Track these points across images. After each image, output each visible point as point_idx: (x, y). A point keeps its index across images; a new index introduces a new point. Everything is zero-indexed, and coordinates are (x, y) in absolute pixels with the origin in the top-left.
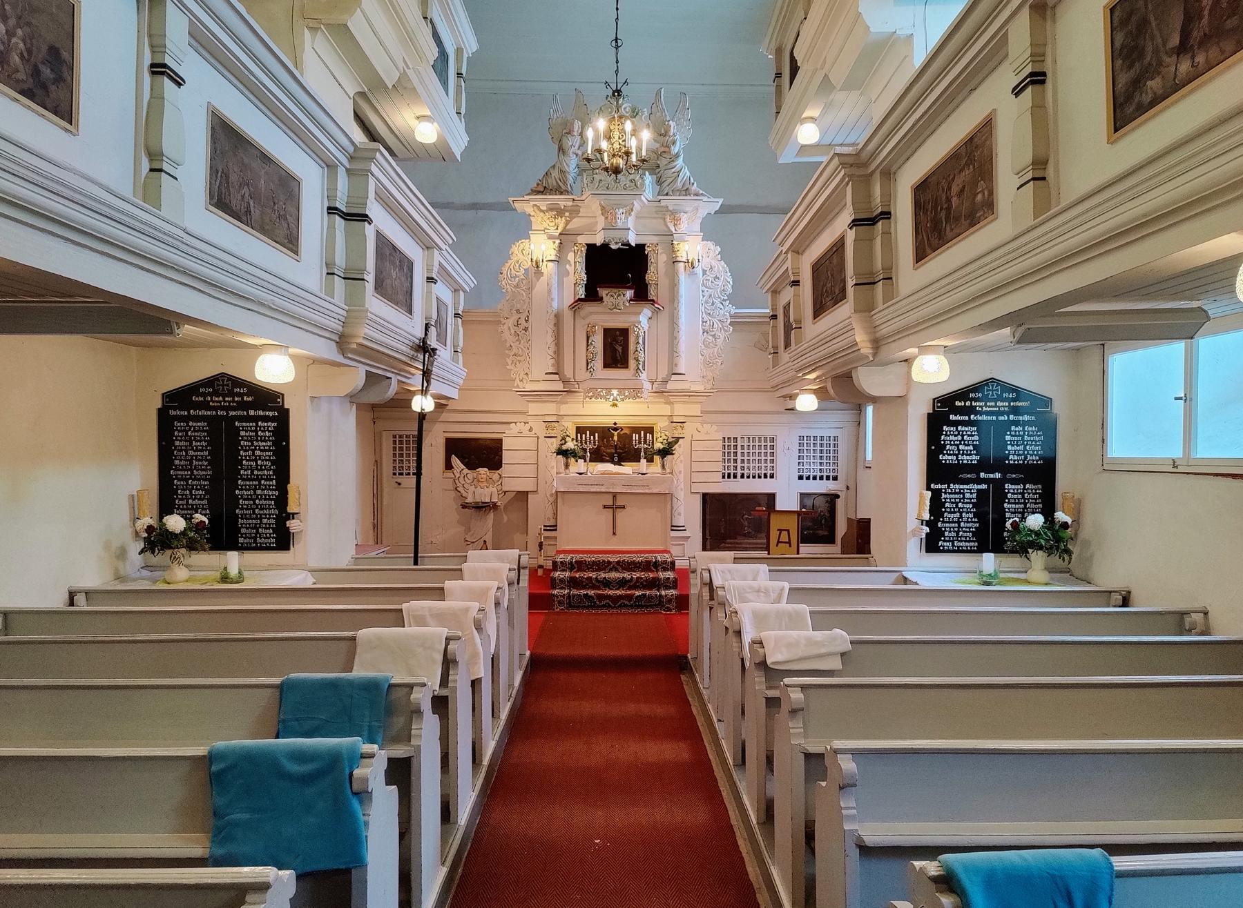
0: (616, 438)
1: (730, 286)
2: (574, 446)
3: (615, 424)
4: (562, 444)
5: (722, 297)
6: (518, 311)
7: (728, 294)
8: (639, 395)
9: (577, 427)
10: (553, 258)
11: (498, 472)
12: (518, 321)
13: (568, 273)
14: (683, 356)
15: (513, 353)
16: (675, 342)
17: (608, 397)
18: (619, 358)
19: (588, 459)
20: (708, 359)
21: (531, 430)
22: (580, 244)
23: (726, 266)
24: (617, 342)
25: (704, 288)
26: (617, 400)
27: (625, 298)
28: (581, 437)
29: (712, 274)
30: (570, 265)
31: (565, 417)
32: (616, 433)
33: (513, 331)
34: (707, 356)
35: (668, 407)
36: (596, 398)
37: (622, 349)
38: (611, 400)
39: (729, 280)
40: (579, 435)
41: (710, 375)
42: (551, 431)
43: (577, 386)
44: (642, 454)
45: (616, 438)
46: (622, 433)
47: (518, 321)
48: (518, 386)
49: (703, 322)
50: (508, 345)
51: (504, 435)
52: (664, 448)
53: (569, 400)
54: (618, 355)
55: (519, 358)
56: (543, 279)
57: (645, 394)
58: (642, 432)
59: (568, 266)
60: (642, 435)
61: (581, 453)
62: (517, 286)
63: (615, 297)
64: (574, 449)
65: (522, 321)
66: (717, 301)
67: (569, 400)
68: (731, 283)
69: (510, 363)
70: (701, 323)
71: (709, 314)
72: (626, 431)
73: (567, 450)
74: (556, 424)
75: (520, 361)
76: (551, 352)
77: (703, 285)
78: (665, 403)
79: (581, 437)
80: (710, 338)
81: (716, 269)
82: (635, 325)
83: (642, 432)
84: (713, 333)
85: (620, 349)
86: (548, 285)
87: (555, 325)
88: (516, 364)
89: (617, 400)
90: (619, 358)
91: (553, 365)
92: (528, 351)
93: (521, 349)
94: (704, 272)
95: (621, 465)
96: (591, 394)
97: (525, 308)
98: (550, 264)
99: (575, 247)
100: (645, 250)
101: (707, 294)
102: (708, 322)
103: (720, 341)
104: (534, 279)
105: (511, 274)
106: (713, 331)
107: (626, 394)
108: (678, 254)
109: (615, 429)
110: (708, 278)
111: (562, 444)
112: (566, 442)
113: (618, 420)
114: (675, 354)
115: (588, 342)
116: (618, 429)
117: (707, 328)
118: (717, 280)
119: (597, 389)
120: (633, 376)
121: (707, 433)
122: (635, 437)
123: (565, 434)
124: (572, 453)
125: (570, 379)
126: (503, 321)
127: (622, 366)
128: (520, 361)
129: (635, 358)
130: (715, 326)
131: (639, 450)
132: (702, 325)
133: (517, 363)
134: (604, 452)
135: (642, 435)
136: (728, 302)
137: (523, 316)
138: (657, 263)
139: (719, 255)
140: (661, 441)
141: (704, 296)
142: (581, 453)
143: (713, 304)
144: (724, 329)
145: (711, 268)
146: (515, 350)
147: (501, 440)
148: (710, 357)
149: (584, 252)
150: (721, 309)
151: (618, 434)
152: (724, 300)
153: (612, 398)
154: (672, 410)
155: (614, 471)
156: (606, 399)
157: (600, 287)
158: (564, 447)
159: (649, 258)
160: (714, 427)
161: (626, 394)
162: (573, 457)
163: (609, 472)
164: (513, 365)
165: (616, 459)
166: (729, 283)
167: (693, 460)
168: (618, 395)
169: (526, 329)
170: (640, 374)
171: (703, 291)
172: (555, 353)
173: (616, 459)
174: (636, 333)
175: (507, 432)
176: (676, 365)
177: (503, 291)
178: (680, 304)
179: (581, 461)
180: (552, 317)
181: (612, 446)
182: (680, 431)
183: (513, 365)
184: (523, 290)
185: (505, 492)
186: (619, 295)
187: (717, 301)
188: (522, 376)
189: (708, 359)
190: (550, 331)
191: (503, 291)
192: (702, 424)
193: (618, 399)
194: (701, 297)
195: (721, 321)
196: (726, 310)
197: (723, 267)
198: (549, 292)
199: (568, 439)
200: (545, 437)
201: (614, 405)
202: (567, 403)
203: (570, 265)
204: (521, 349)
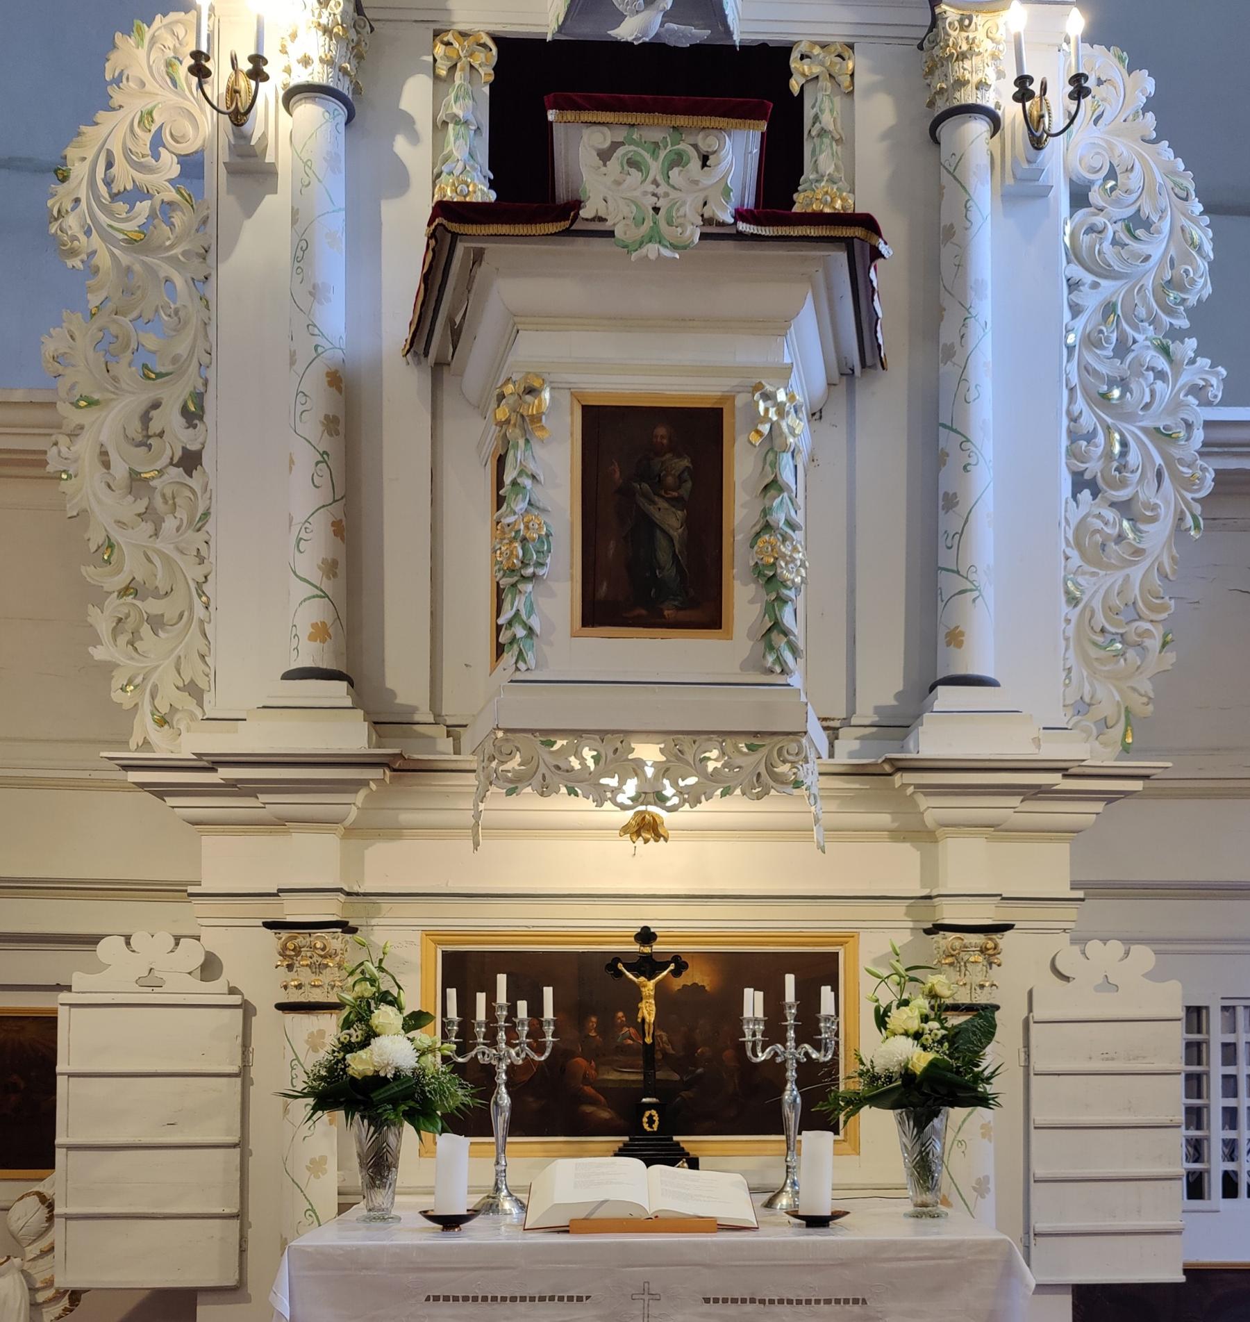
0: (648, 1011)
1: (1203, 266)
2: (422, 1053)
3: (646, 936)
4: (348, 1047)
5: (1166, 319)
6: (148, 374)
7: (1192, 300)
8: (783, 769)
9: (445, 954)
10: (318, 74)
11: (38, 1187)
12: (146, 419)
13: (399, 180)
14: (989, 592)
15: (121, 581)
16: (949, 522)
17: (613, 782)
18: (668, 572)
19: (501, 1122)
20: (1100, 620)
21: (210, 968)
22: (464, 35)
23: (1181, 165)
24: (658, 483)
25: (1077, 272)
26: (660, 799)
27: (709, 179)
28: (466, 1008)
29: (1118, 203)
30: (414, 138)
31: (385, 904)
32: (649, 987)
33: (120, 470)
34: (1097, 604)
35: (908, 854)
36: (545, 790)
37: (688, 523)
38: (621, 798)
39: (1197, 234)
40: (452, 993)
41: (1108, 699)
42: (305, 976)
43: (446, 744)
44: (791, 1093)
45: (648, 1011)
46: (678, 983)
47: (146, 419)
48: (146, 745)
49: (1073, 436)
50: (97, 539)
51: (64, 997)
52: (933, 1064)
53: (405, 817)
54: (664, 556)
55: (152, 606)
56: (276, 206)
57: (810, 773)
58: (790, 980)
59: (401, 145)
60: (790, 995)
61: (459, 1096)
62: (138, 243)
63: (655, 167)
64: (418, 1074)
65: (170, 419)
66: (1144, 337)
67: (405, 817)
68: (1208, 248)
69: (102, 622)
70: (1064, 442)
71: (1105, 396)
72: (696, 976)
73: (376, 1081)
74: (335, 940)
75: (157, 623)
76: (310, 561)
77: (1075, 255)
78: (898, 835)
79: (466, 1008)
80: (1110, 514)
81: (1134, 180)
82: (758, 387)
83: (790, 980)
84: (1122, 494)
85: (672, 521)
86: (294, 221)
87: (331, 424)
88: (135, 636)
89: (660, 799)
90: (668, 572)
91: (320, 633)
92: (194, 573)
93: (167, 559)
94: (1079, 198)
95: (672, 1156)
96: (514, 764)
97: (182, 348)
98: (309, 112)
99: (440, 50)
100: (789, 74)
101: (1091, 301)
102: (1101, 438)
103: (1157, 535)
104: (229, 203)
105: (108, 183)
106: (1123, 484)
107: (711, 766)
108: (969, 70)
109: (648, 965)
110: (1099, 220)
111: (348, 1047)
112: (371, 1035)
113: (659, 918)
114: (948, 583)
115: (500, 484)
116: (664, 966)
117: (1093, 468)
118: (1140, 232)
119: (547, 736)
120: (745, 666)
121: (1108, 985)
122: (753, 1003)
123: (367, 990)
124: (407, 1096)
125: (414, 710)
126: (75, 417)
127: (683, 615)
128: (157, 623)
129: (758, 570)
130: (1134, 458)
131: (775, 1069)
132: (1072, 453)
133: (146, 629)
134: (586, 1080)
135: (790, 995)
136: (1192, 343)
137: (174, 396)
138: (845, 141)
139: (1150, 116)
140: (915, 1025)
141: (1076, 310)
142: (459, 1096)
143: (1122, 349)
144: (1178, 479)
145: (1112, 174)
146: (132, 567)
147: (48, 1023)
148: (1109, 610)
149: (486, 74)
150: (1160, 375)
151: (661, 993)
152: (1177, 334)
153: (631, 787)
154: (929, 869)
155: (651, 1210)
156: (601, 796)
157: (560, 107)
158: (360, 1064)
159: (808, 114)
160: (1144, 956)
161: (711, 766)
162: (412, 1117)
163: (622, 1213)
164: (123, 639)
165: (651, 1121)
166: (1199, 249)
167: (1038, 1117)
168: (664, 770)
169: (190, 461)
170: (788, 656)
171: (1073, 285)
172: (330, 568)
173: (651, 1121)
174: (765, 428)
175: (78, 980)
176: (955, 638)
177: (76, 262)
178: (975, 328)
179: (453, 1145)
180: (315, 383)
181: (622, 1049)
182: (976, 974)
183: (123, 639)
184: (173, 261)
185: (75, 1296)
186: (678, 160)
187: (1144, 337)
188: (169, 695)
189: (1100, 620)
190: (305, 458)
191: (76, 262)
192: (1080, 940)
193: (669, 791)
194: (1067, 315)
195: (1162, 436)
196: (1184, 379)
197: (1170, 173)
198: (302, 251)
199: (385, 1017)
200: (282, 1007)
201: (646, 828)
202: (394, 832)
203: (414, 138)
204: (167, 559)
